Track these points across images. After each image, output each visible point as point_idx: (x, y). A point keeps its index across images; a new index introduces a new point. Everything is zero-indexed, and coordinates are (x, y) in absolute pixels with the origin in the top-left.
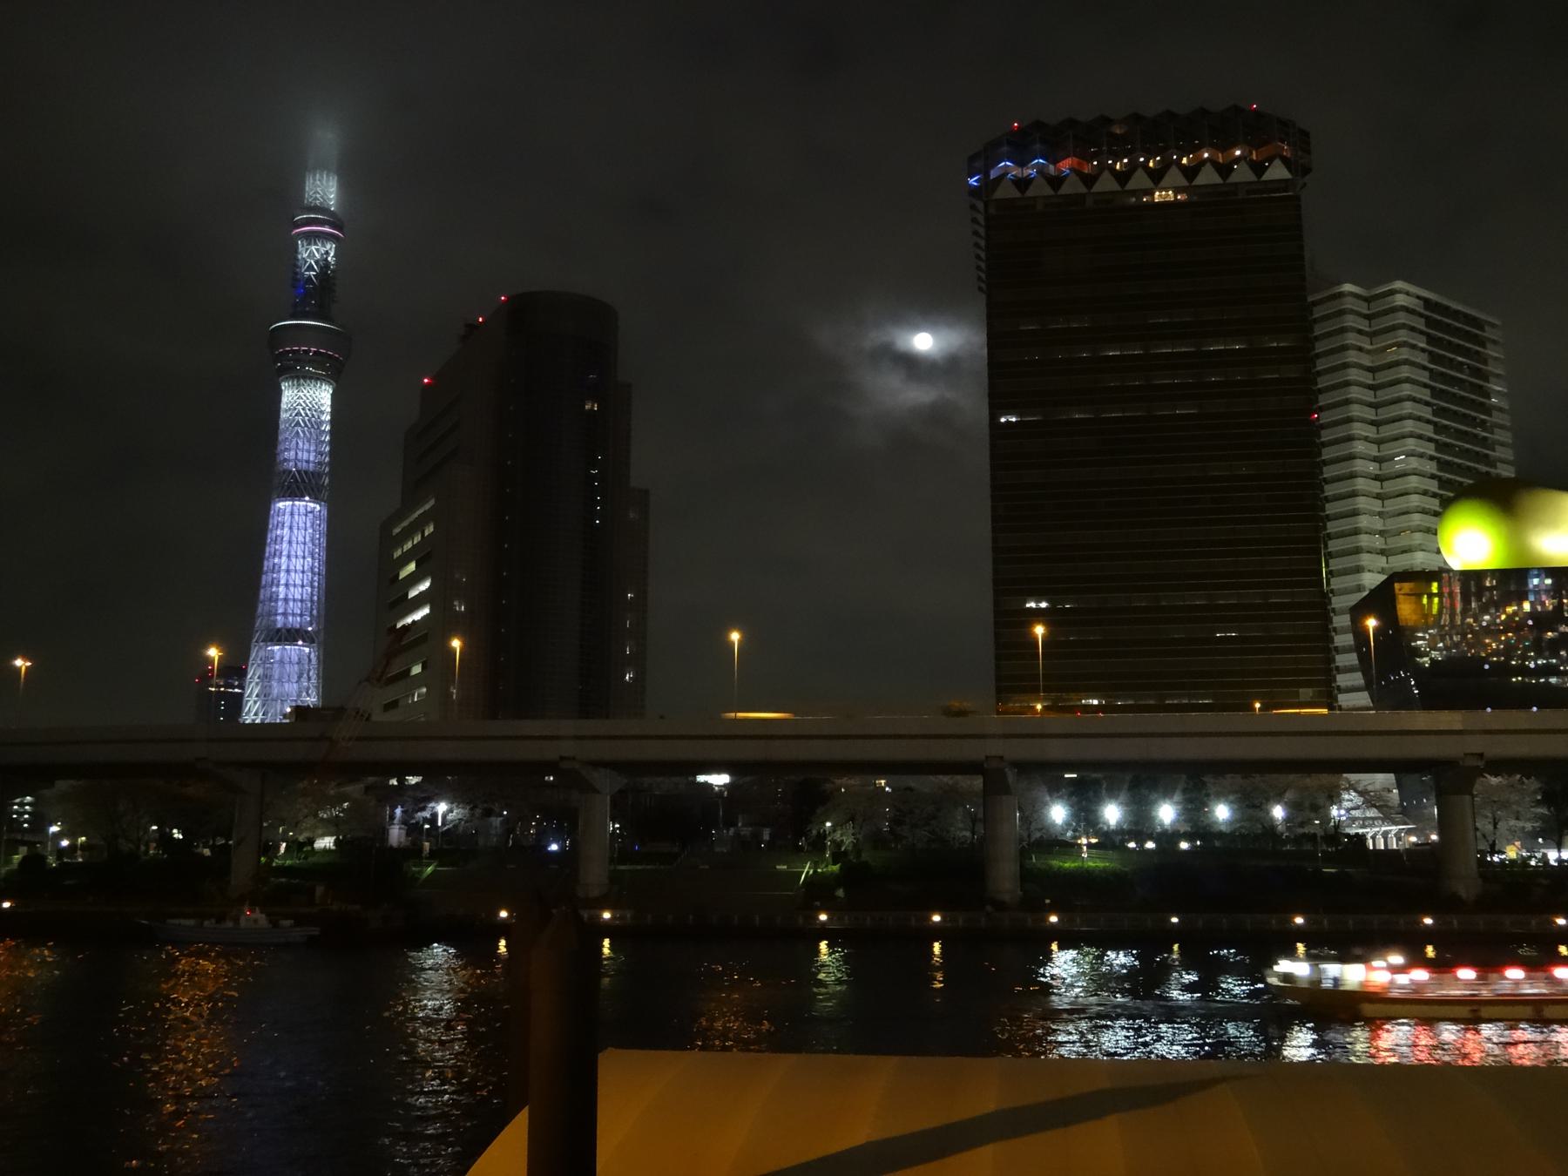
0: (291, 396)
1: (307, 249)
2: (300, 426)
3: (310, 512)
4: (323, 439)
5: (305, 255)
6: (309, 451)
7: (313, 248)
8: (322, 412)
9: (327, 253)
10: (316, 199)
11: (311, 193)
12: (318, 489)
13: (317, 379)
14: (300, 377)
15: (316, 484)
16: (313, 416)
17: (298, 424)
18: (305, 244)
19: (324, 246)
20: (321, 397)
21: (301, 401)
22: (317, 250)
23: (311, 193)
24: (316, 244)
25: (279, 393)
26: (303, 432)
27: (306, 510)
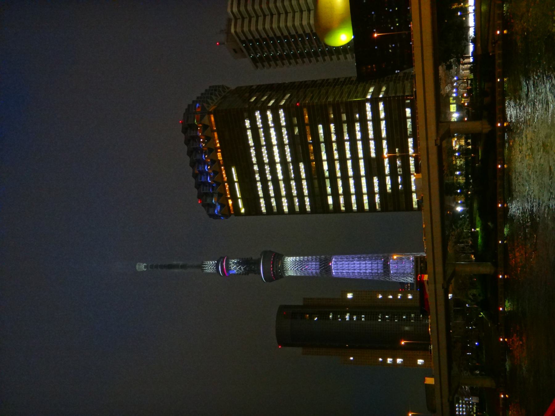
0: (291, 272)
1: (233, 270)
2: (302, 268)
3: (336, 263)
4: (306, 259)
5: (236, 271)
6: (312, 265)
7: (232, 268)
8: (296, 260)
9: (233, 263)
10: (213, 268)
11: (212, 270)
12: (326, 260)
13: (283, 263)
14: (283, 269)
15: (324, 261)
16: (298, 264)
17: (301, 269)
18: (231, 271)
19: (231, 264)
20: (289, 260)
21: (292, 269)
22: (233, 267)
23: (212, 270)
24: (231, 267)
25: (290, 276)
26: (304, 267)
27: (335, 264)
